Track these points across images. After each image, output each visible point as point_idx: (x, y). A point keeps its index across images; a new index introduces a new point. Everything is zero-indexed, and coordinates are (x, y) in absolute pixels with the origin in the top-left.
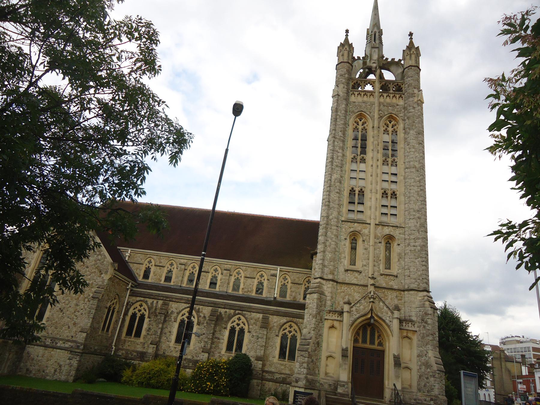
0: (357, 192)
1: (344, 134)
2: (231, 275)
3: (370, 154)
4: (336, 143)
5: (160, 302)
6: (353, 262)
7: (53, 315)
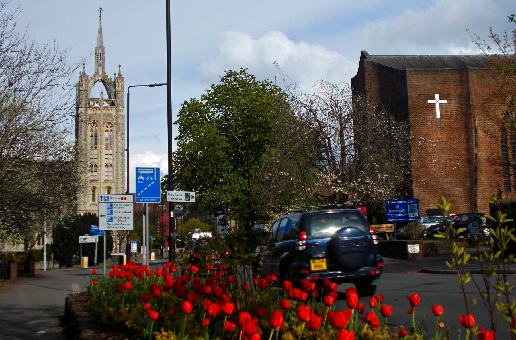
1: (86, 136)
3: (99, 146)
6: (93, 200)
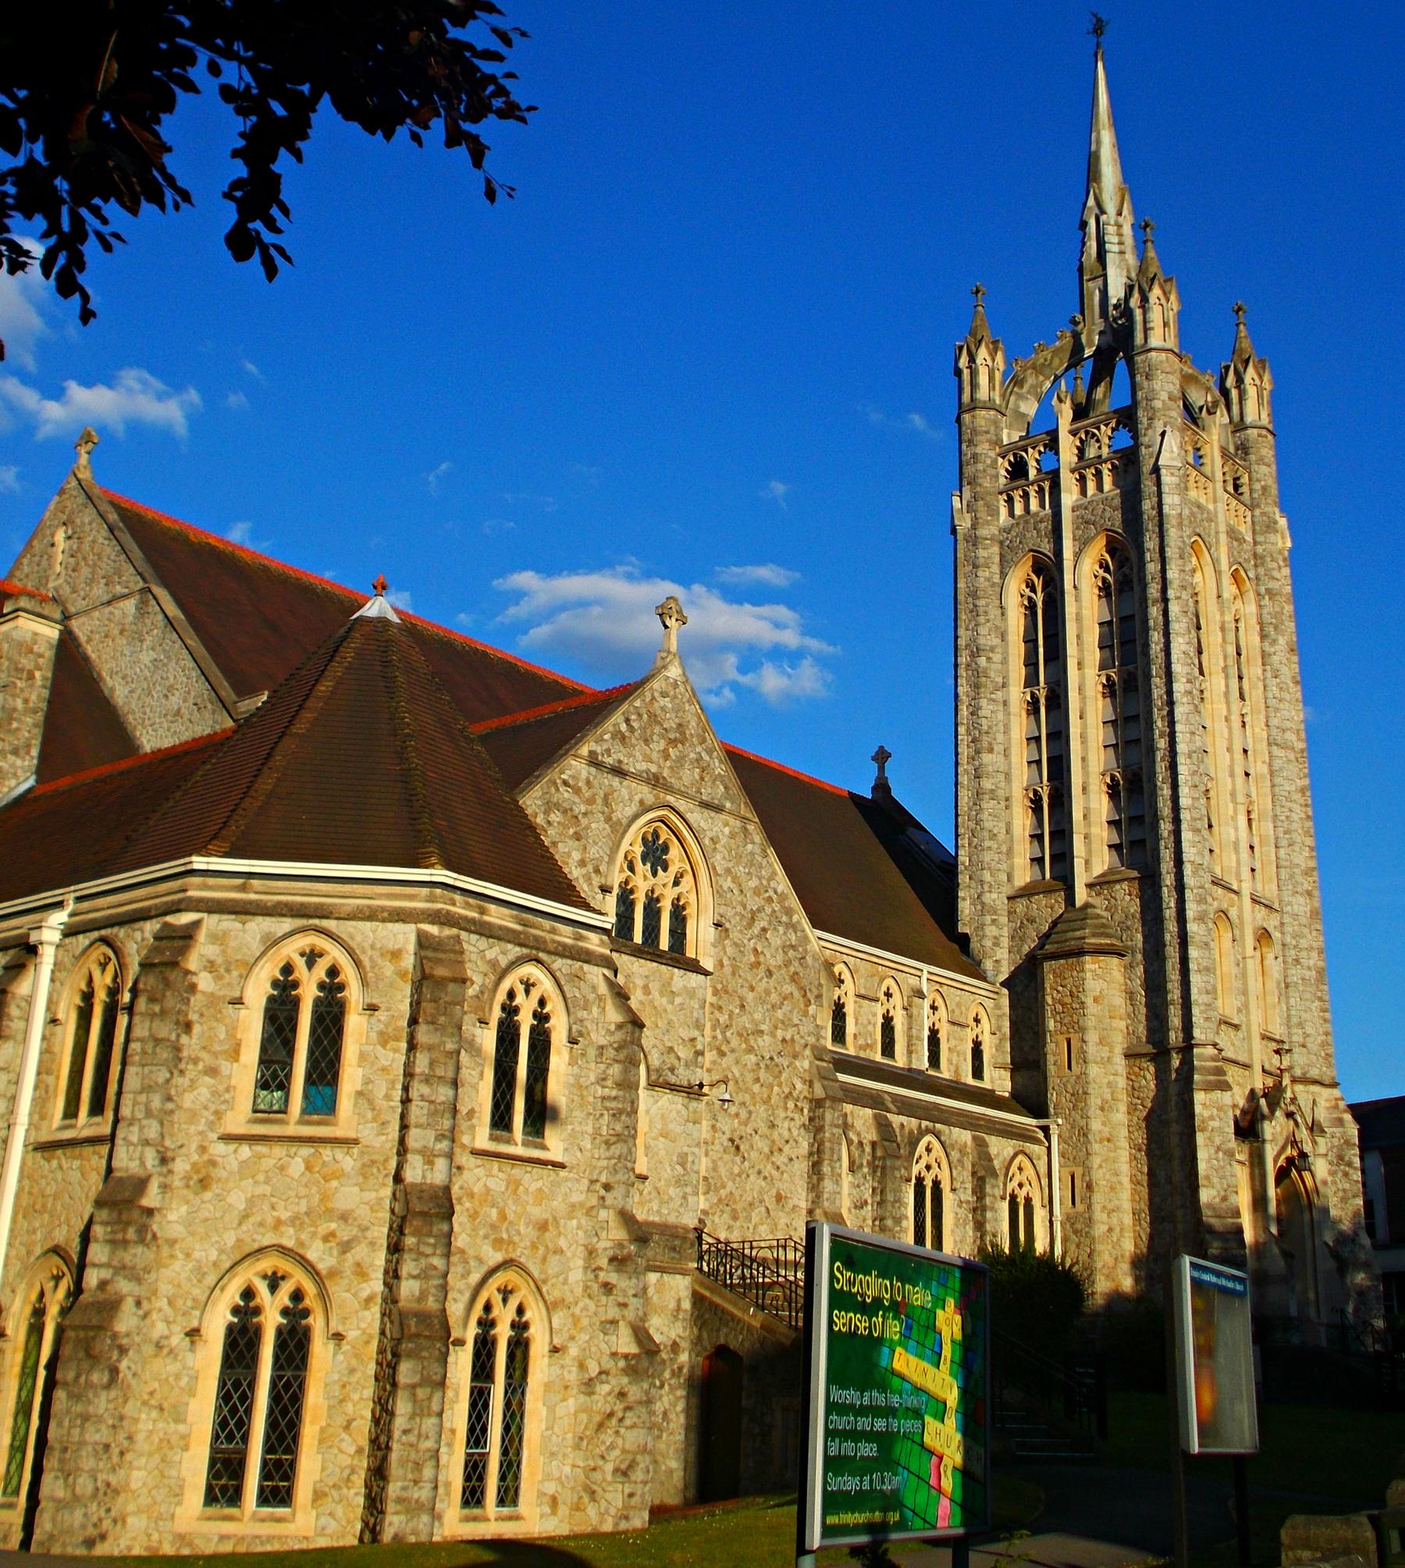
7: (715, 1169)
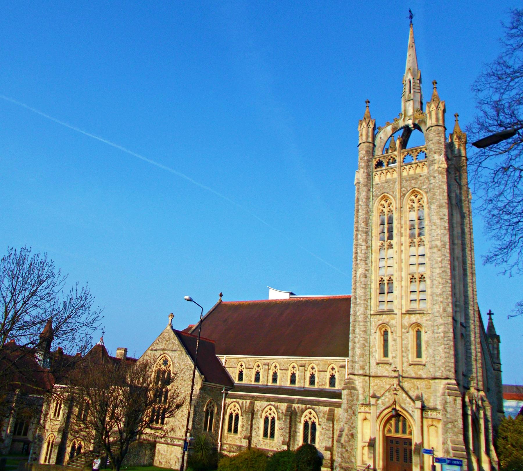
0: (386, 282)
2: (305, 370)
4: (359, 236)
5: (248, 401)
6: (386, 355)
